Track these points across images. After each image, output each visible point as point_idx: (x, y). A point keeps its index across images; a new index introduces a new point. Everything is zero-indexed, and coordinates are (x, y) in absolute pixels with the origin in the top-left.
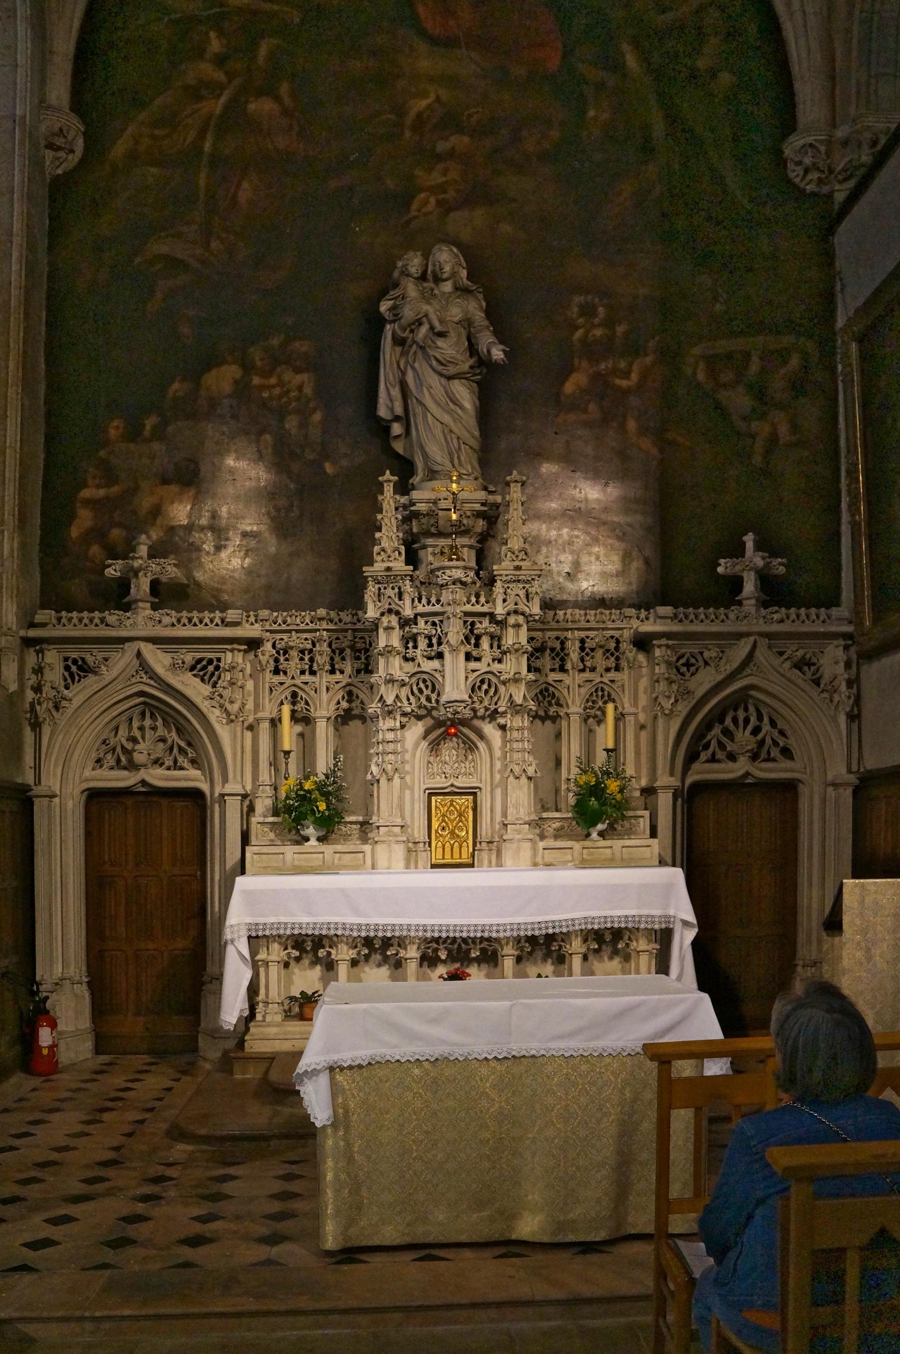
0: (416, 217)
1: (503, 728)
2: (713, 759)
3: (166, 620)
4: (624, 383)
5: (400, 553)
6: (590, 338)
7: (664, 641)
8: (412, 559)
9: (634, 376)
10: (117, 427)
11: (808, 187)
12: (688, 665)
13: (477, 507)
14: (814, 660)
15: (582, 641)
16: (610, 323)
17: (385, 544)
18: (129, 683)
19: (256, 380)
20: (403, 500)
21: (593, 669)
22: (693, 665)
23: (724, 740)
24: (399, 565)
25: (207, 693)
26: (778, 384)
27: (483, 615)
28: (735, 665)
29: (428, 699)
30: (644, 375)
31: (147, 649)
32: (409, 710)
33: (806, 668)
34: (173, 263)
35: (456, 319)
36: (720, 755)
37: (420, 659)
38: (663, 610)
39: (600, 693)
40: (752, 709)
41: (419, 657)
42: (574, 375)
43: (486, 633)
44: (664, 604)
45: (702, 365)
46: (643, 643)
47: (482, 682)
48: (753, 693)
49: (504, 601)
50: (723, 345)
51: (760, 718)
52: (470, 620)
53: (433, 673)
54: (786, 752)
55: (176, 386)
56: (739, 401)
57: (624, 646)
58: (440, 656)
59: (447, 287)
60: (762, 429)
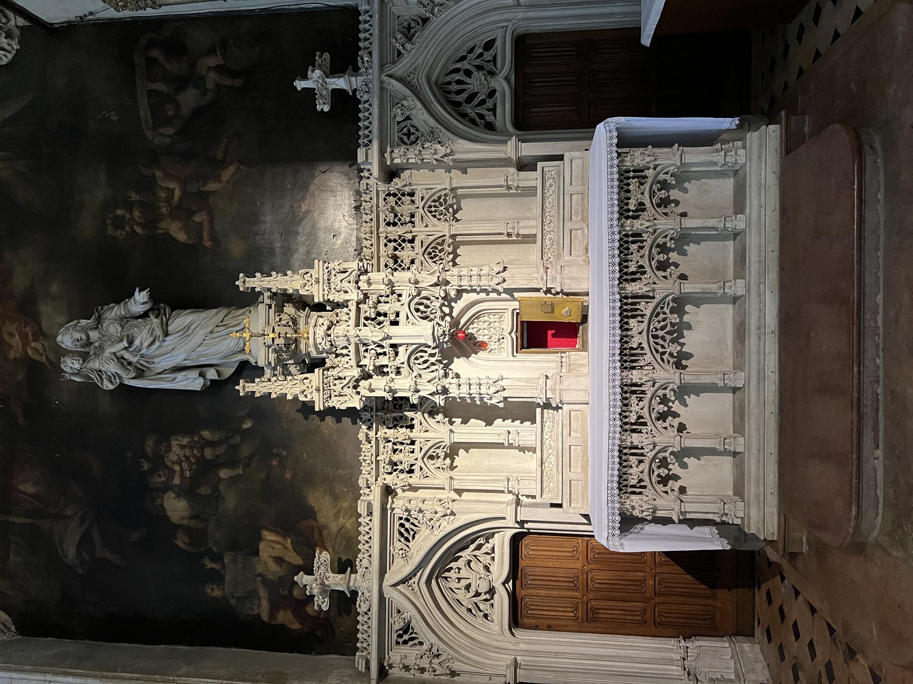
0: (47, 358)
1: (460, 292)
2: (493, 110)
3: (365, 563)
4: (177, 193)
5: (306, 378)
6: (142, 221)
7: (387, 155)
8: (313, 364)
9: (172, 185)
10: (212, 589)
11: (15, 47)
12: (409, 134)
13: (272, 311)
14: (405, 24)
15: (388, 224)
16: (130, 206)
17: (297, 391)
18: (418, 593)
19: (177, 481)
20: (268, 372)
21: (412, 216)
22: (409, 130)
23: (476, 101)
25: (428, 531)
26: (174, 67)
27: (358, 310)
28: (407, 92)
29: (432, 355)
30: (171, 177)
31: (392, 577)
32: (442, 372)
33: (412, 31)
34: (85, 542)
35: (119, 329)
36: (489, 104)
37: (397, 363)
38: (361, 158)
39: (433, 209)
40: (448, 79)
41: (395, 364)
42: (171, 232)
43: (375, 308)
44: (355, 157)
45: (161, 130)
46: (390, 174)
47: (417, 310)
48: (433, 79)
49: (346, 292)
50: (145, 114)
51: (457, 71)
52: (362, 320)
53: (409, 352)
54: (489, 45)
55: (180, 544)
56: (189, 99)
57: (393, 190)
58: (394, 346)
59: (94, 335)
60: (212, 78)
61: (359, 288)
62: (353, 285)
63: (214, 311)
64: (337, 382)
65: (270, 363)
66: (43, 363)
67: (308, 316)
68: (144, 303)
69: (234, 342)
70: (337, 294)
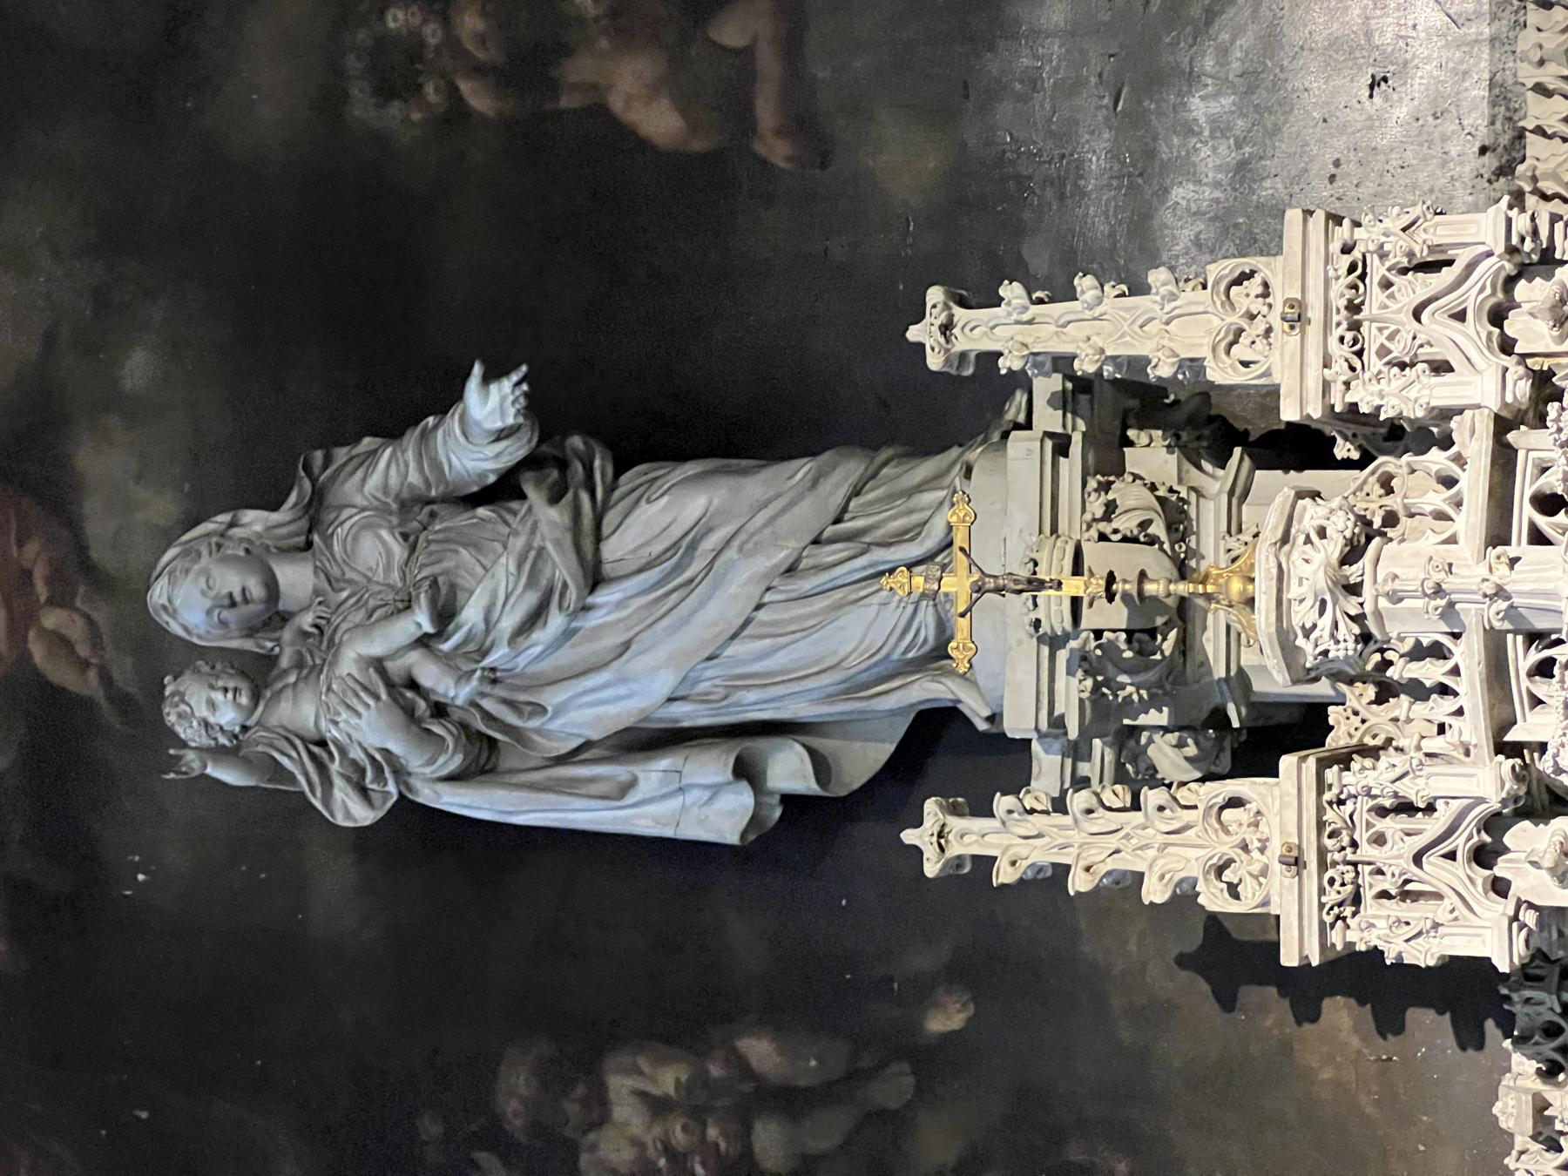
5: (1235, 802)
8: (1266, 736)
13: (1071, 467)
17: (1188, 861)
20: (1047, 767)
24: (1283, 795)
27: (1504, 458)
35: (399, 551)
42: (616, 104)
52: (1524, 513)
59: (295, 578)
61: (1507, 346)
62: (1476, 330)
63: (803, 468)
64: (1391, 826)
65: (1058, 723)
66: (87, 704)
67: (1239, 494)
68: (501, 435)
69: (893, 617)
70: (1396, 379)
